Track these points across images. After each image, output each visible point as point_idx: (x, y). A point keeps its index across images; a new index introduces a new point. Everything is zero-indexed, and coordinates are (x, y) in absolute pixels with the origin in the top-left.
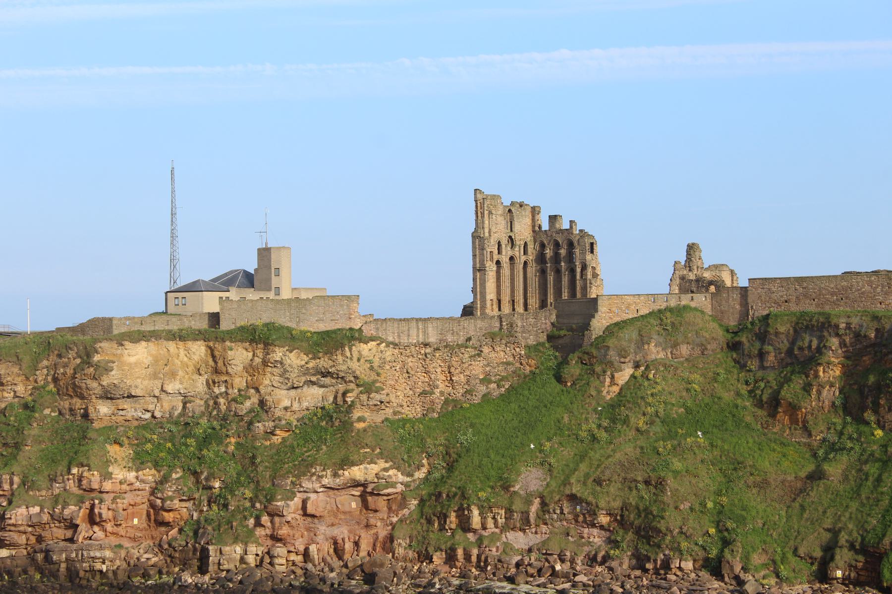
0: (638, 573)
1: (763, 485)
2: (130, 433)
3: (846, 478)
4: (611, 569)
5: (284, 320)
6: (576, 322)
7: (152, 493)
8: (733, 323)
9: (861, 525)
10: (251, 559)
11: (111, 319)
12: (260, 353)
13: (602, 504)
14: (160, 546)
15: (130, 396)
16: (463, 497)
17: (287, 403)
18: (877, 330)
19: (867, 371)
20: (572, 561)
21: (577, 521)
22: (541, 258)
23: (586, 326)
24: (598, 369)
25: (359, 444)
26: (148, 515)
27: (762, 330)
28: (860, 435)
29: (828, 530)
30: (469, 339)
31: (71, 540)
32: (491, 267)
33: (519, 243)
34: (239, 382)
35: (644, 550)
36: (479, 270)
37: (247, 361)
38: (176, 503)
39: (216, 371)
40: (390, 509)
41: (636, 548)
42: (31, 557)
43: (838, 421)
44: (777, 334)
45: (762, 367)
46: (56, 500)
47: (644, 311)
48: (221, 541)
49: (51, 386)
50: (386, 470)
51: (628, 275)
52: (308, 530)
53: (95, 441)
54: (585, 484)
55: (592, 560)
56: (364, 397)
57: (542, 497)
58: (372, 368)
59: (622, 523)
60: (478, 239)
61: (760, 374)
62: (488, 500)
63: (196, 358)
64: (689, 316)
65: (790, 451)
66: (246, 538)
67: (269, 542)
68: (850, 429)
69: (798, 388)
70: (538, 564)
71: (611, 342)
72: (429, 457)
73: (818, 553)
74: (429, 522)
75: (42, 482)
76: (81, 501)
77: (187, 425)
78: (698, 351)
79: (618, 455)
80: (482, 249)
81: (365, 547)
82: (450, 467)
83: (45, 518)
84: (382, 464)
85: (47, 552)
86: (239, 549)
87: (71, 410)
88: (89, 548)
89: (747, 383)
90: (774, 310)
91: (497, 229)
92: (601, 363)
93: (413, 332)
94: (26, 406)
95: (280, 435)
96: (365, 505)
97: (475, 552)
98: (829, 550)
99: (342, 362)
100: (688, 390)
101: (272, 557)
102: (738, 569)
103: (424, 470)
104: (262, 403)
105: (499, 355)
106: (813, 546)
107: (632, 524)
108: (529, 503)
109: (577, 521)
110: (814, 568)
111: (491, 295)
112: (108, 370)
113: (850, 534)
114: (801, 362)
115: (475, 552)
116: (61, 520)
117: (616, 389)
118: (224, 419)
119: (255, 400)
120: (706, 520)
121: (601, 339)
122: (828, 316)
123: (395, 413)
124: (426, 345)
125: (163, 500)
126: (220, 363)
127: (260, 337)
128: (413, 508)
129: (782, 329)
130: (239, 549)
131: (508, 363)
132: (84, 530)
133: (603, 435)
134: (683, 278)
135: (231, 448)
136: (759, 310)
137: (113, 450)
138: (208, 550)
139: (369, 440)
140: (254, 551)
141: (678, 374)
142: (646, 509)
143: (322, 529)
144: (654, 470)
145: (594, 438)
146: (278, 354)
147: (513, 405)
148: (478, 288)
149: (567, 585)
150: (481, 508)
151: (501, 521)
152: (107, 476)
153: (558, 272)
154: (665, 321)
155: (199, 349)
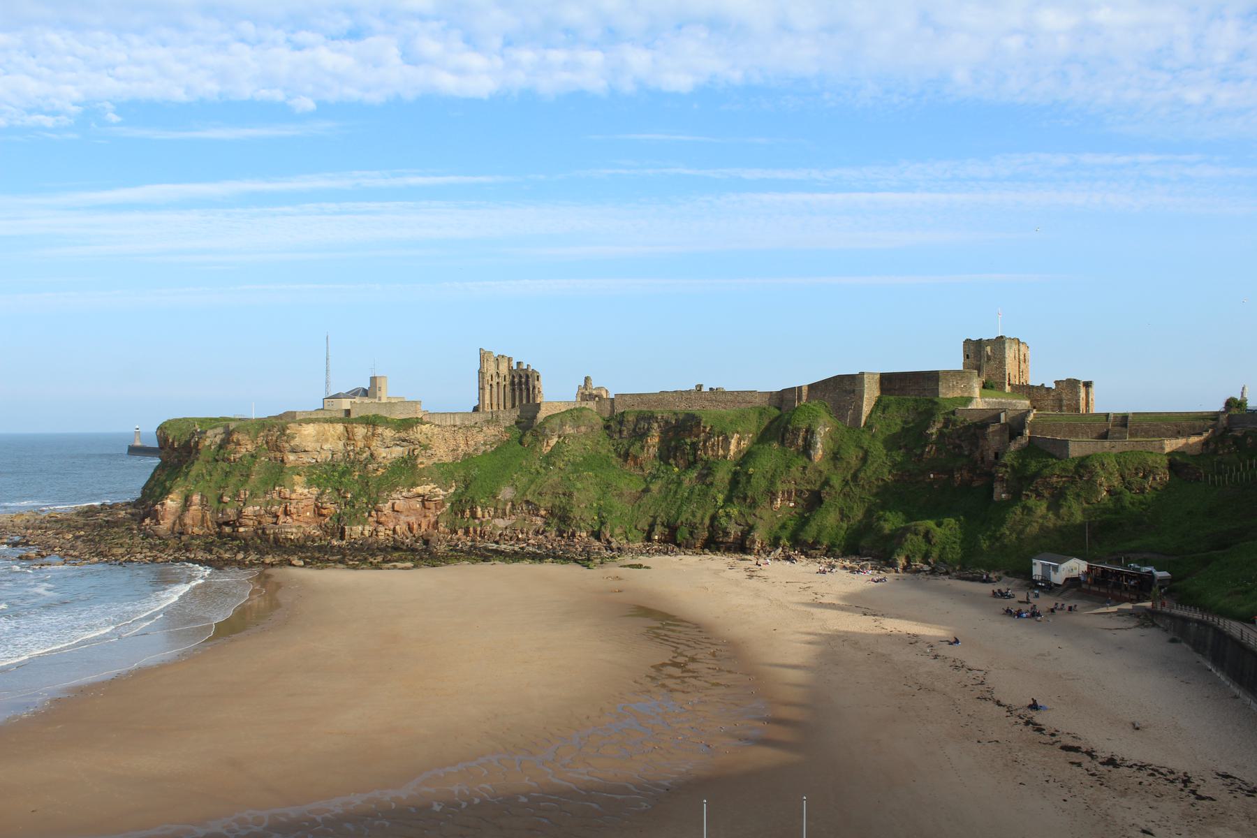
1: (621, 495)
5: (383, 413)
6: (530, 414)
8: (607, 416)
9: (667, 514)
10: (366, 533)
19: (671, 440)
22: (512, 383)
23: (535, 417)
25: (421, 476)
27: (622, 420)
32: (488, 388)
34: (360, 444)
36: (482, 388)
38: (328, 505)
39: (349, 439)
42: (255, 532)
46: (268, 503)
48: (351, 524)
51: (556, 393)
55: (537, 533)
60: (481, 373)
64: (585, 412)
66: (364, 523)
71: (547, 425)
73: (647, 528)
75: (261, 493)
76: (281, 503)
77: (333, 466)
81: (424, 526)
82: (467, 487)
84: (433, 485)
85: (264, 529)
91: (491, 368)
94: (252, 456)
98: (652, 526)
104: (372, 455)
105: (491, 431)
111: (487, 401)
114: (640, 435)
127: (371, 422)
130: (360, 528)
132: (282, 519)
133: (543, 471)
136: (619, 410)
137: (296, 478)
139: (426, 473)
141: (581, 441)
143: (403, 518)
145: (538, 473)
146: (380, 430)
148: (481, 398)
152: (294, 491)
153: (521, 390)
154: (574, 415)
155: (340, 428)
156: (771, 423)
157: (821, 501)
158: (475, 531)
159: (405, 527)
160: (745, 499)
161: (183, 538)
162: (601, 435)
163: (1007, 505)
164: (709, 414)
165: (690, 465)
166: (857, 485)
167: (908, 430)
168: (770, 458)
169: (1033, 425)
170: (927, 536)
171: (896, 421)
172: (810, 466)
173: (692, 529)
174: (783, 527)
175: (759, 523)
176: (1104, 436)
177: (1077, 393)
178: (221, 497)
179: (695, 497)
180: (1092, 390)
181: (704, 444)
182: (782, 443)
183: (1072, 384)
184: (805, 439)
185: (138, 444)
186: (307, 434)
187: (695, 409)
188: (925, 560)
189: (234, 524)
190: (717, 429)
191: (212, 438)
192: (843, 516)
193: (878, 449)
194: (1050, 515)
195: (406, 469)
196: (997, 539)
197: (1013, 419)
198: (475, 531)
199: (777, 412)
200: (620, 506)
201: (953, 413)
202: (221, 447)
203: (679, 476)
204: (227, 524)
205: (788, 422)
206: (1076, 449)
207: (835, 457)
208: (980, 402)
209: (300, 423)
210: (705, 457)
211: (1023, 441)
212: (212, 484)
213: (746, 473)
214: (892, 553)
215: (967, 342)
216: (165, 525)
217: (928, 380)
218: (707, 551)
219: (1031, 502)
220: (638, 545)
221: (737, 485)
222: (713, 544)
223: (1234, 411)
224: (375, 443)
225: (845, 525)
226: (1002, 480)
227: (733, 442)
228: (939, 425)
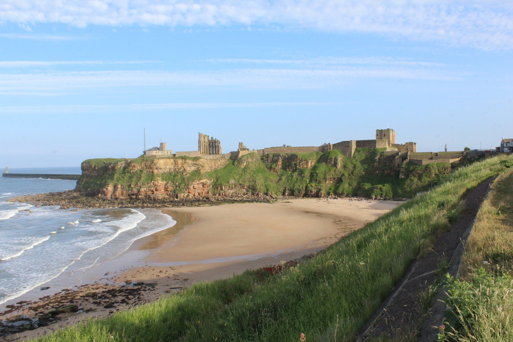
1: (272, 181)
5: (187, 155)
7: (165, 185)
8: (261, 155)
9: (290, 186)
19: (286, 163)
22: (209, 145)
23: (238, 156)
27: (267, 156)
31: (153, 194)
34: (180, 166)
35: (254, 192)
42: (146, 196)
46: (149, 187)
55: (244, 194)
59: (249, 188)
81: (204, 193)
82: (217, 180)
85: (149, 196)
91: (202, 140)
94: (140, 171)
95: (188, 175)
96: (203, 186)
104: (184, 169)
105: (223, 161)
106: (282, 190)
114: (276, 161)
116: (151, 190)
121: (240, 159)
127: (184, 158)
132: (155, 192)
136: (266, 153)
140: (186, 195)
141: (254, 164)
143: (197, 191)
146: (187, 161)
152: (158, 183)
153: (213, 147)
155: (172, 160)
156: (321, 157)
157: (342, 181)
160: (316, 180)
161: (118, 200)
162: (261, 162)
163: (404, 179)
164: (300, 154)
165: (294, 171)
166: (353, 175)
167: (368, 158)
168: (322, 168)
169: (410, 156)
170: (381, 189)
171: (363, 156)
172: (337, 170)
174: (330, 189)
175: (322, 188)
176: (431, 159)
177: (413, 146)
178: (130, 185)
179: (298, 181)
180: (416, 145)
181: (299, 163)
182: (326, 163)
183: (411, 144)
184: (334, 161)
185: (7, 172)
186: (161, 163)
187: (293, 152)
188: (381, 196)
190: (304, 159)
191: (121, 166)
192: (350, 185)
193: (359, 165)
194: (419, 181)
195: (197, 174)
196: (403, 189)
197: (403, 154)
199: (322, 153)
200: (272, 185)
201: (383, 152)
202: (125, 168)
203: (291, 174)
204: (133, 195)
205: (328, 156)
206: (425, 162)
207: (345, 167)
208: (389, 149)
209: (159, 159)
211: (407, 160)
213: (316, 173)
214: (370, 195)
215: (377, 130)
216: (109, 196)
217: (372, 143)
219: (412, 178)
220: (281, 197)
221: (313, 176)
222: (307, 195)
223: (467, 151)
225: (351, 188)
226: (402, 172)
227: (310, 163)
228: (378, 156)
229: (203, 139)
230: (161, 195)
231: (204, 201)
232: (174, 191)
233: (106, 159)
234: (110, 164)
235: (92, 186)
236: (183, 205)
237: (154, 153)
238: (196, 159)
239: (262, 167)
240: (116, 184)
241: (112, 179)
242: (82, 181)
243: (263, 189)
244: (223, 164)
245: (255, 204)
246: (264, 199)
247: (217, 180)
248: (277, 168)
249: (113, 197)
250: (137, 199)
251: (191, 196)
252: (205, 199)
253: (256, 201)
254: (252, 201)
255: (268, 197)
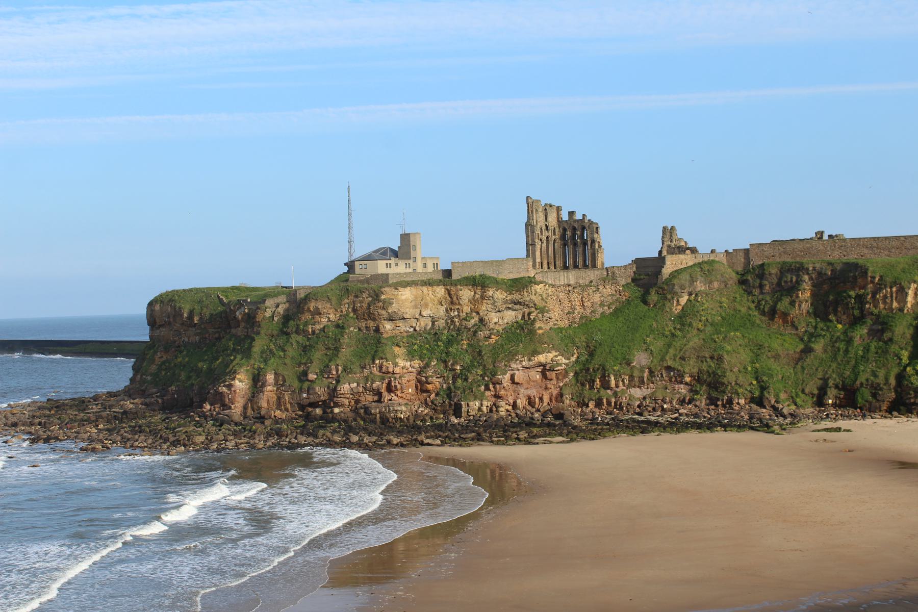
0: (713, 407)
2: (405, 340)
3: (825, 351)
4: (696, 406)
5: (490, 273)
7: (419, 373)
8: (740, 269)
9: (841, 375)
10: (484, 409)
11: (387, 275)
12: (479, 292)
13: (687, 370)
14: (426, 403)
15: (404, 319)
16: (603, 368)
17: (496, 320)
18: (832, 271)
20: (671, 402)
21: (671, 381)
22: (563, 237)
23: (659, 272)
24: (669, 296)
26: (416, 387)
27: (761, 272)
28: (828, 327)
29: (821, 379)
30: (591, 282)
31: (379, 401)
32: (538, 242)
33: (551, 228)
34: (466, 309)
35: (714, 394)
37: (471, 297)
39: (452, 303)
40: (558, 379)
41: (709, 394)
42: (355, 411)
43: (812, 320)
44: (770, 274)
45: (762, 293)
46: (367, 379)
47: (691, 264)
49: (352, 315)
50: (556, 356)
52: (514, 391)
53: (386, 344)
54: (675, 360)
55: (682, 402)
56: (540, 316)
57: (650, 369)
58: (542, 299)
61: (761, 297)
62: (619, 371)
63: (439, 296)
64: (716, 266)
65: (787, 338)
67: (494, 399)
68: (821, 325)
69: (787, 304)
70: (653, 405)
71: (675, 281)
72: (578, 348)
73: (816, 392)
74: (583, 385)
75: (356, 368)
78: (723, 285)
79: (691, 343)
80: (533, 232)
81: (546, 399)
82: (591, 354)
83: (361, 389)
84: (554, 353)
85: (367, 409)
86: (477, 403)
87: (367, 327)
88: (393, 405)
89: (753, 302)
90: (766, 261)
92: (670, 293)
93: (562, 278)
94: (338, 326)
97: (613, 400)
99: (526, 297)
100: (721, 307)
101: (497, 407)
102: (773, 402)
103: (575, 356)
104: (481, 320)
105: (608, 290)
106: (812, 387)
107: (705, 381)
108: (643, 372)
109: (671, 381)
110: (815, 399)
112: (391, 304)
113: (835, 380)
114: (792, 290)
115: (613, 400)
117: (680, 307)
118: (459, 330)
119: (476, 319)
120: (749, 376)
122: (802, 264)
123: (555, 325)
124: (569, 285)
125: (426, 378)
126: (455, 298)
127: (479, 283)
128: (570, 377)
129: (773, 271)
131: (613, 295)
132: (386, 396)
133: (679, 333)
134: (669, 246)
135: (465, 347)
136: (756, 261)
137: (396, 349)
138: (461, 405)
141: (716, 299)
142: (713, 372)
143: (522, 391)
144: (715, 350)
145: (673, 335)
146: (491, 292)
147: (621, 319)
149: (677, 415)
150: (615, 376)
151: (627, 382)
152: (396, 365)
153: (575, 245)
155: (440, 291)
158: (609, 403)
159: (525, 402)
161: (268, 422)
162: (738, 291)
164: (875, 264)
173: (875, 391)
178: (305, 374)
179: (871, 356)
181: (874, 296)
187: (852, 258)
189: (326, 405)
190: (889, 279)
191: (273, 309)
195: (523, 334)
198: (609, 403)
200: (780, 371)
203: (845, 332)
204: (314, 405)
209: (396, 286)
210: (876, 311)
212: (288, 361)
216: (237, 410)
218: (895, 413)
220: (809, 410)
224: (484, 308)
229: (541, 216)
230: (404, 404)
231: (549, 425)
232: (449, 393)
233: (225, 290)
234: (240, 304)
235: (183, 376)
236: (479, 439)
237: (381, 267)
238: (520, 285)
239: (744, 310)
240: (259, 369)
241: (247, 353)
242: (152, 361)
243: (748, 383)
244: (609, 299)
245: (720, 435)
246: (751, 418)
247: (591, 354)
248: (794, 312)
249: (249, 412)
250: (328, 418)
251: (504, 408)
252: (550, 419)
253: (725, 427)
254: (710, 427)
255: (765, 412)
